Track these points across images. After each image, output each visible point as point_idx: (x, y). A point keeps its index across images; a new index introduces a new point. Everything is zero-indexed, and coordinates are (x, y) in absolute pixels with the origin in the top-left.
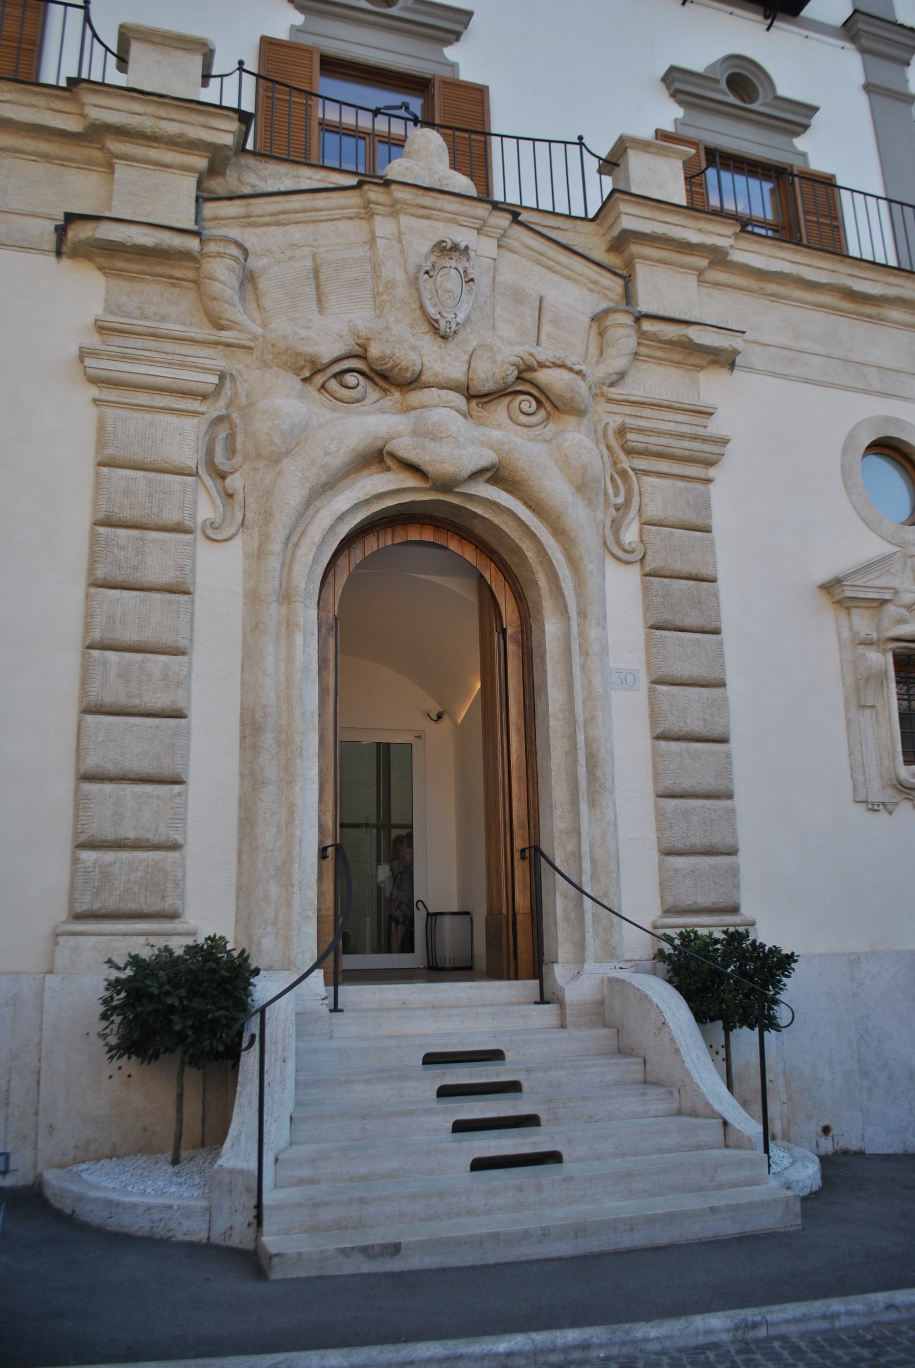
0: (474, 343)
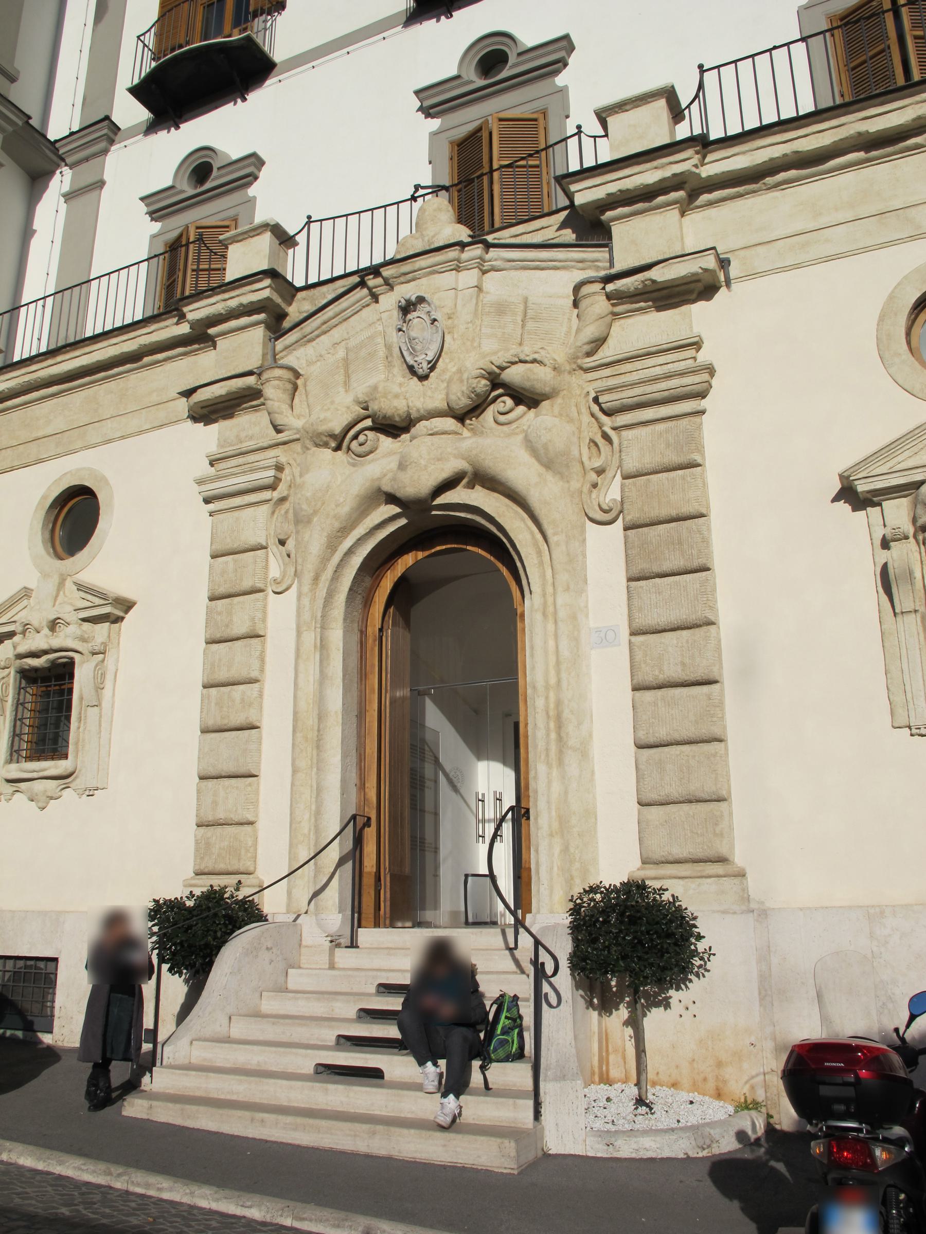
0: (454, 369)
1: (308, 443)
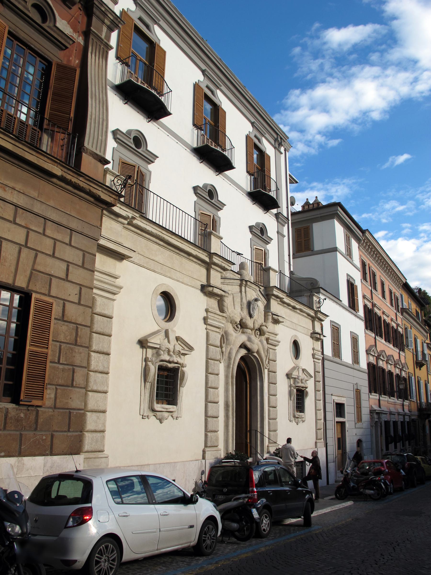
1: (229, 321)
